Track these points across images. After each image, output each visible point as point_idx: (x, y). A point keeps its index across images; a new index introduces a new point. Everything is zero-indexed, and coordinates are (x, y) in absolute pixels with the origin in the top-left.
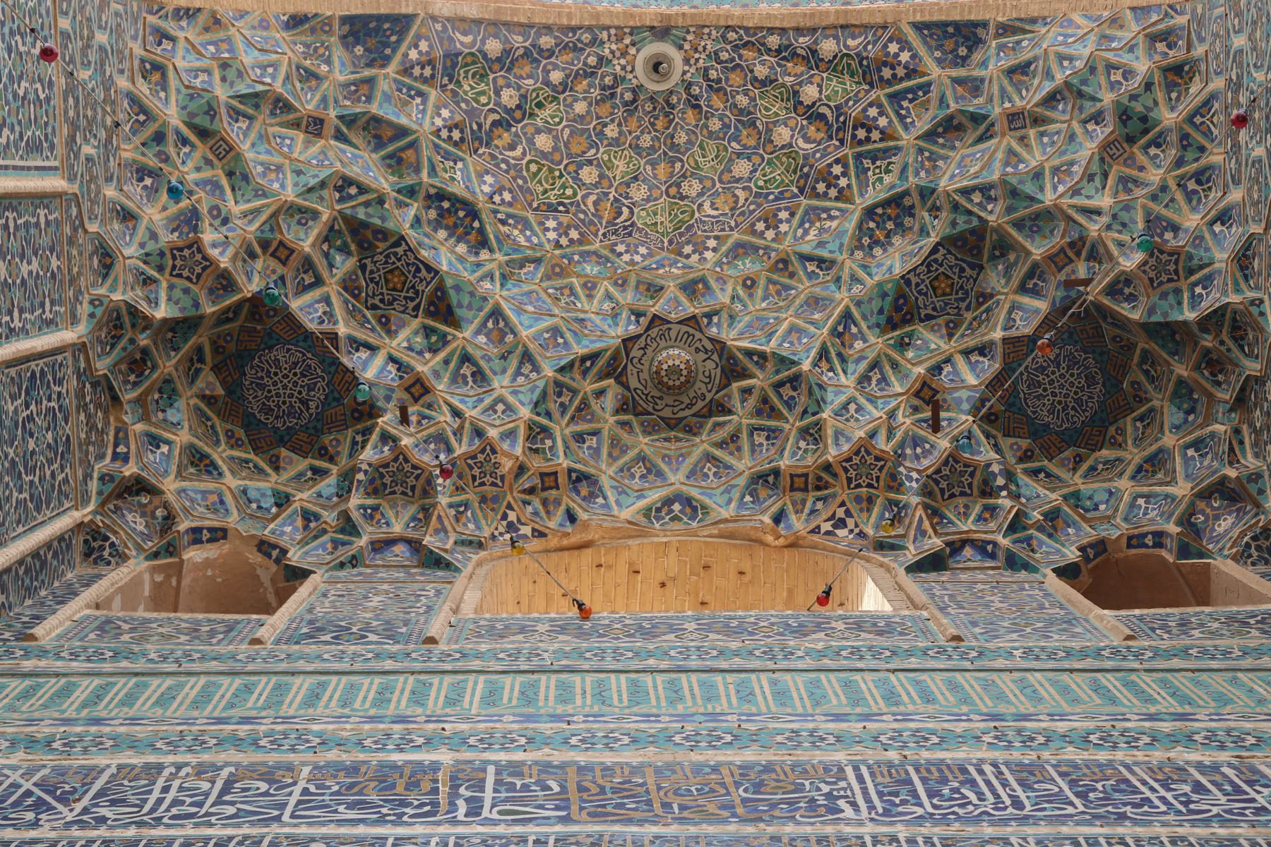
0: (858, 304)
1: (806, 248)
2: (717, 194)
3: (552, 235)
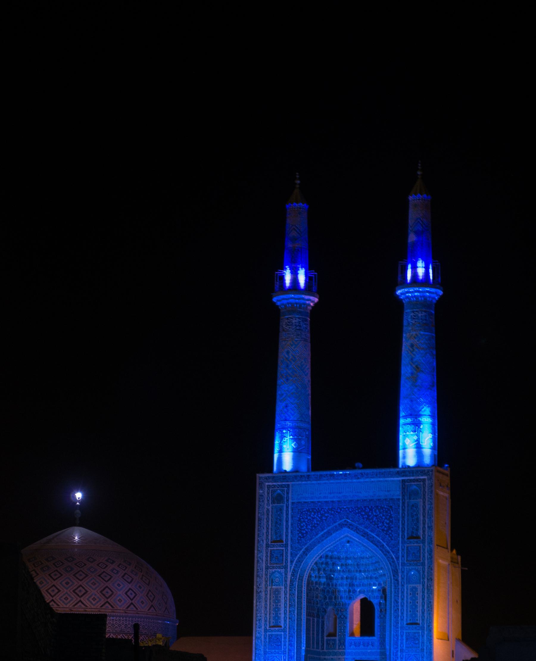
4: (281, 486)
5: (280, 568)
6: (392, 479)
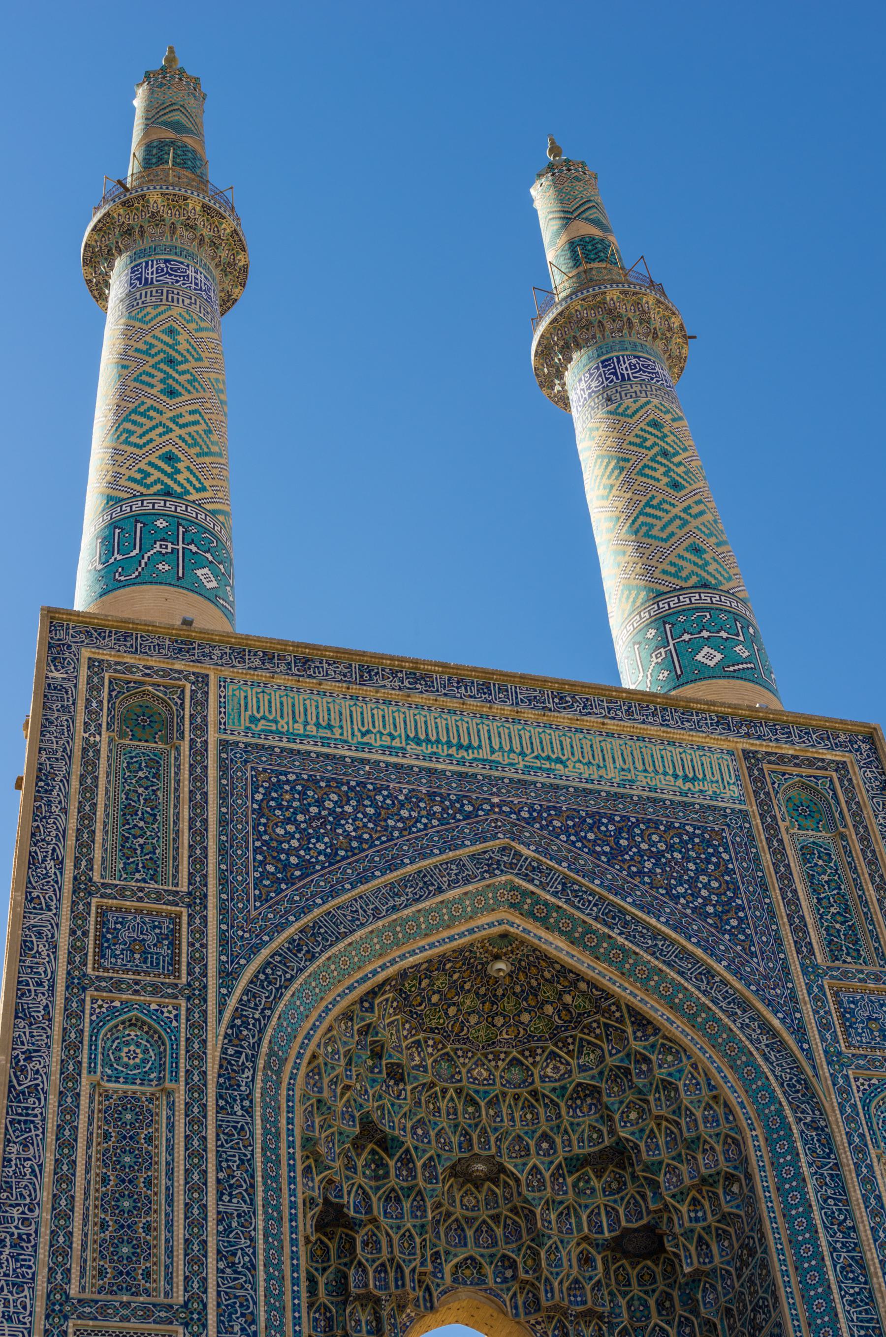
0: (566, 1159)
1: (547, 1093)
2: (510, 1026)
3: (430, 1050)
4: (166, 673)
5: (156, 990)
6: (698, 738)
